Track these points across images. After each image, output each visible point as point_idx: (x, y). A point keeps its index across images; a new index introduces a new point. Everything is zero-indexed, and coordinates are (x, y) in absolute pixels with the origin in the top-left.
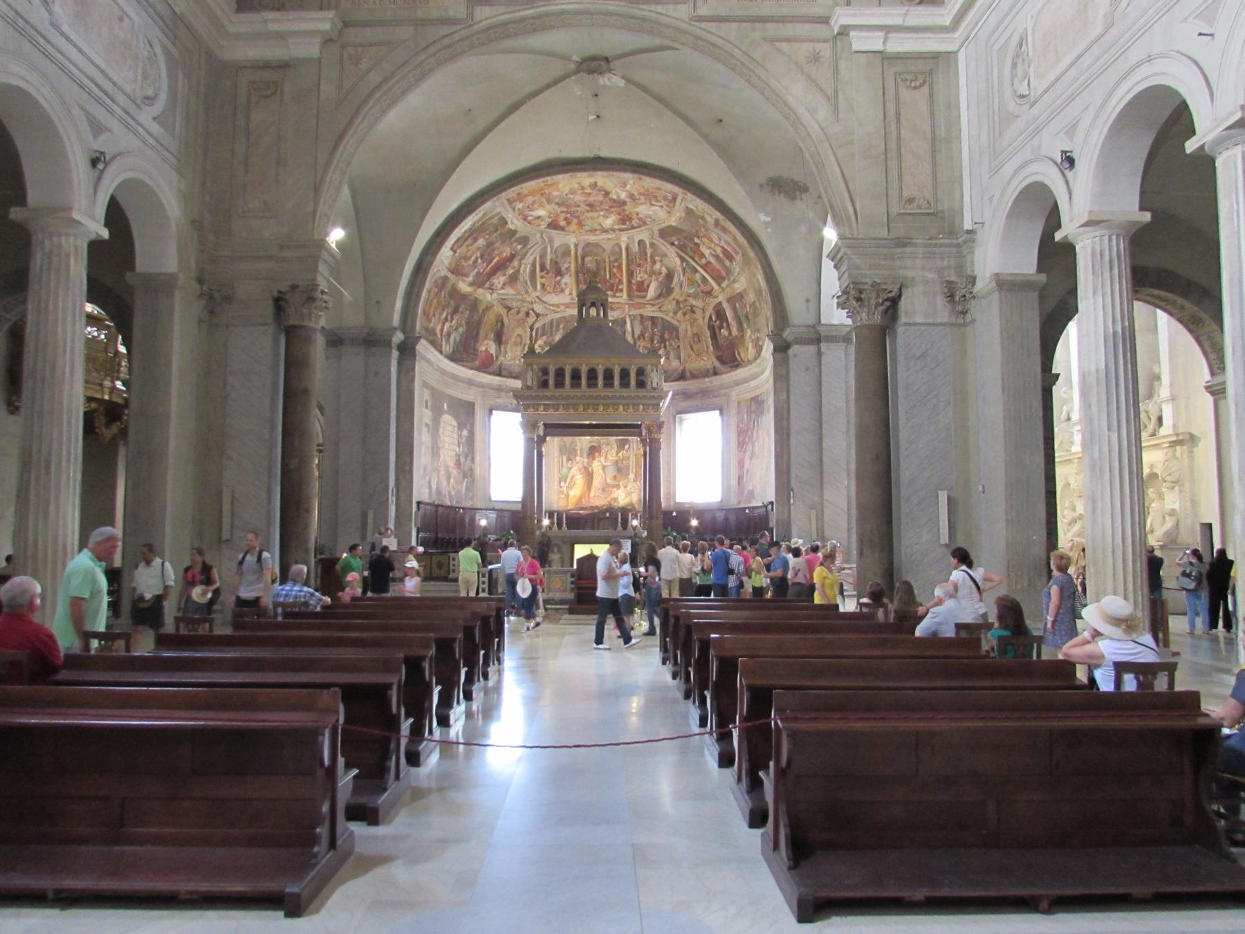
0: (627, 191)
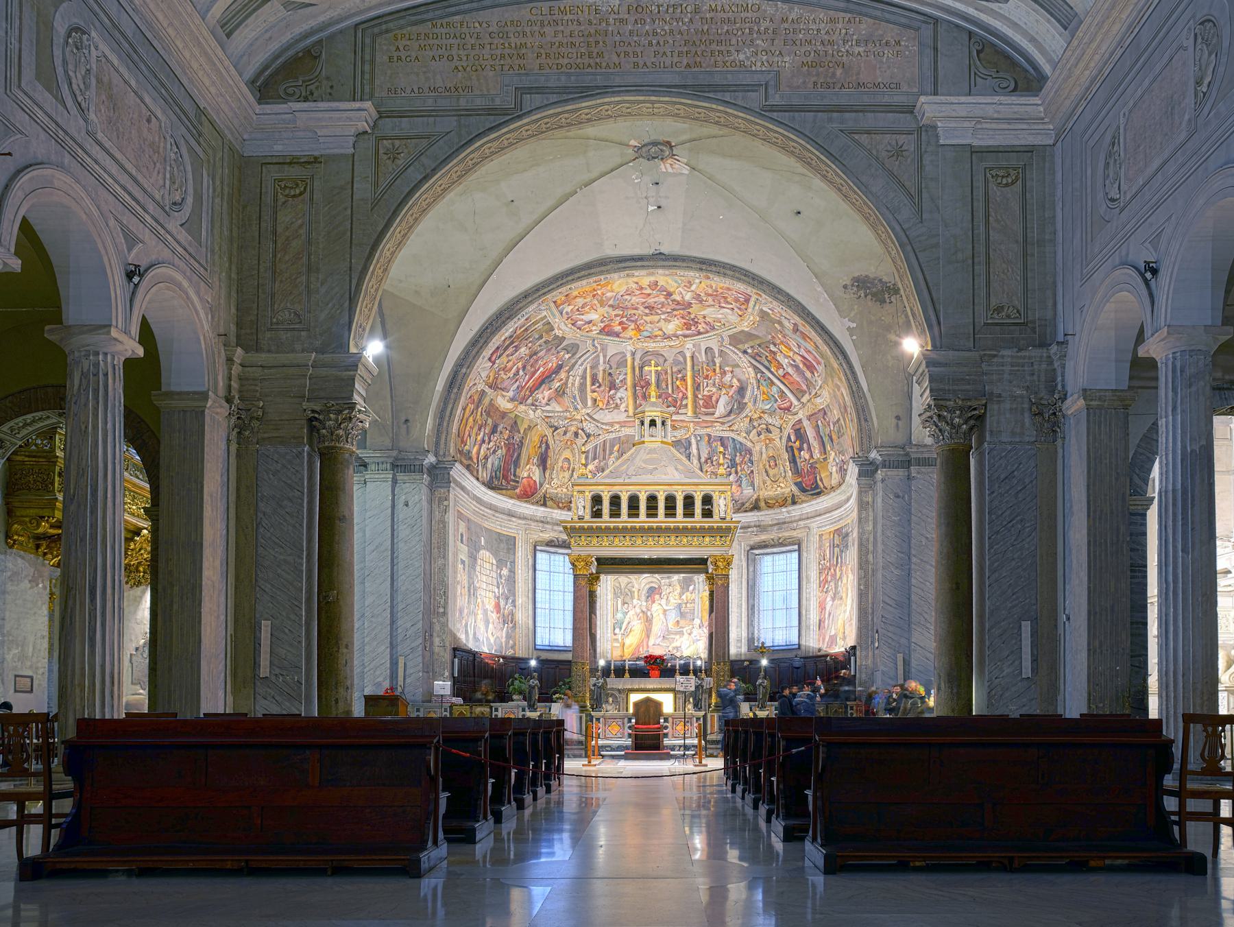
0: (692, 291)
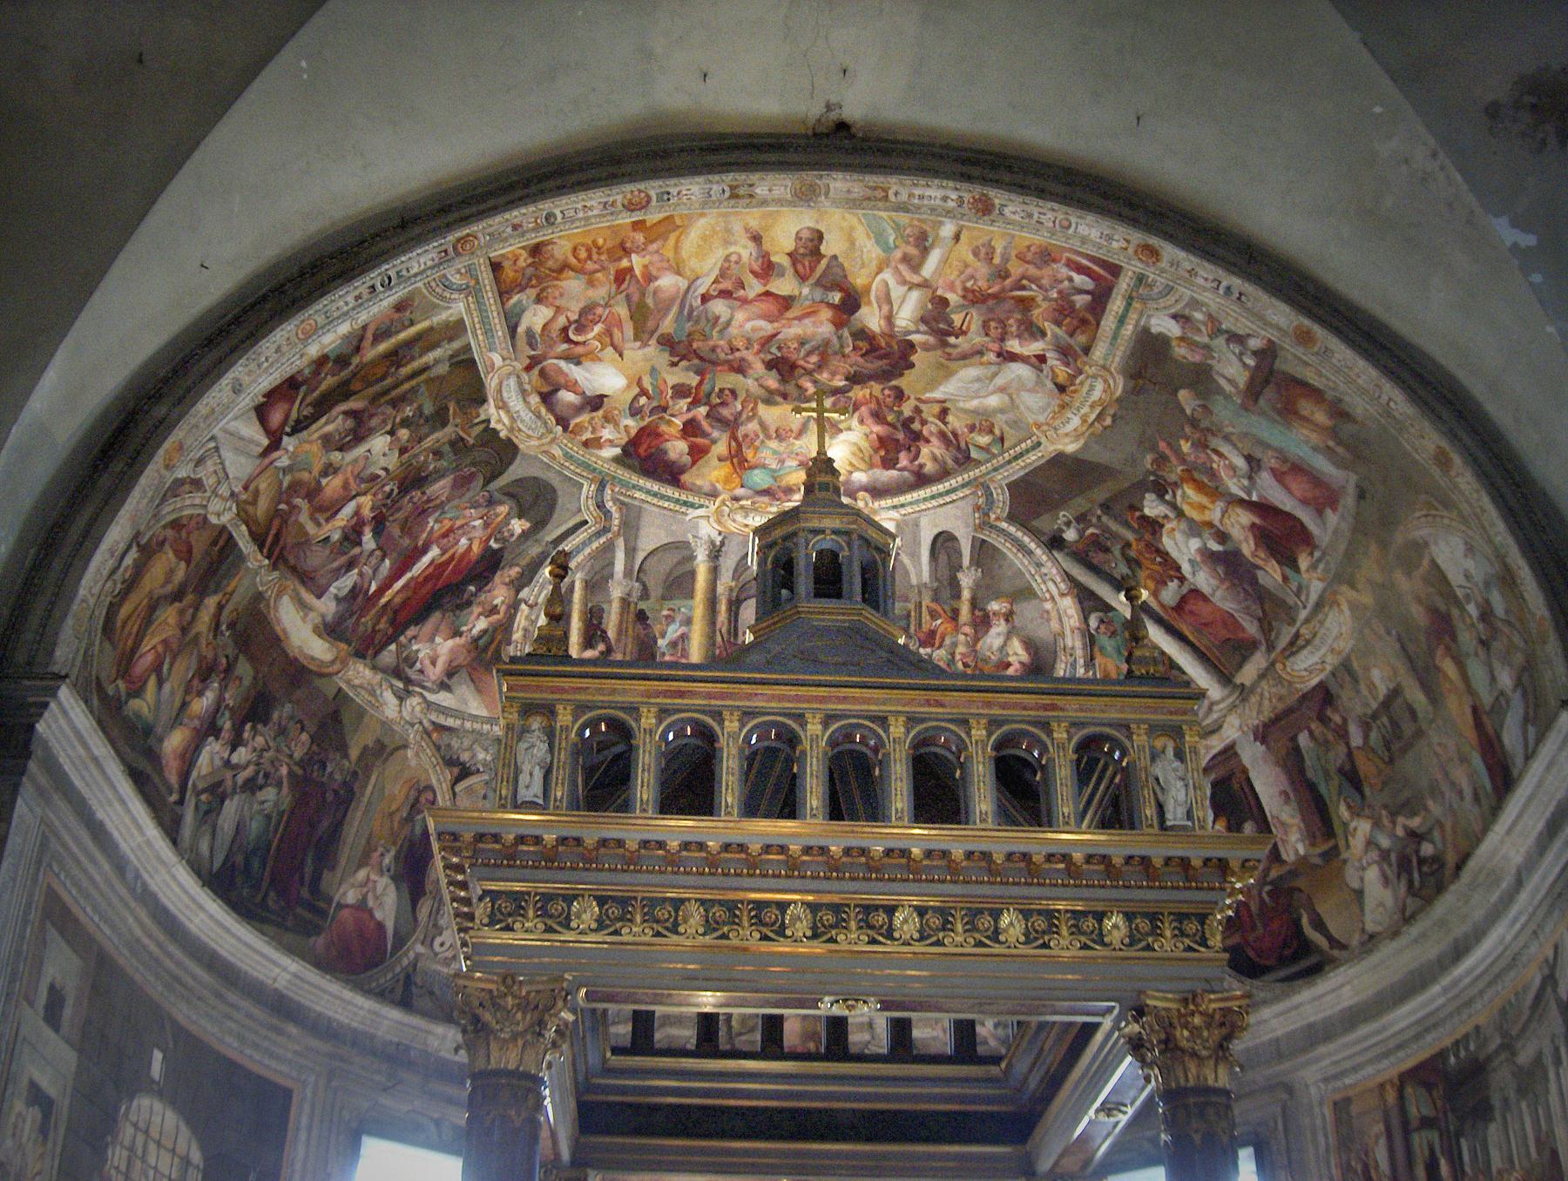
0: (925, 285)
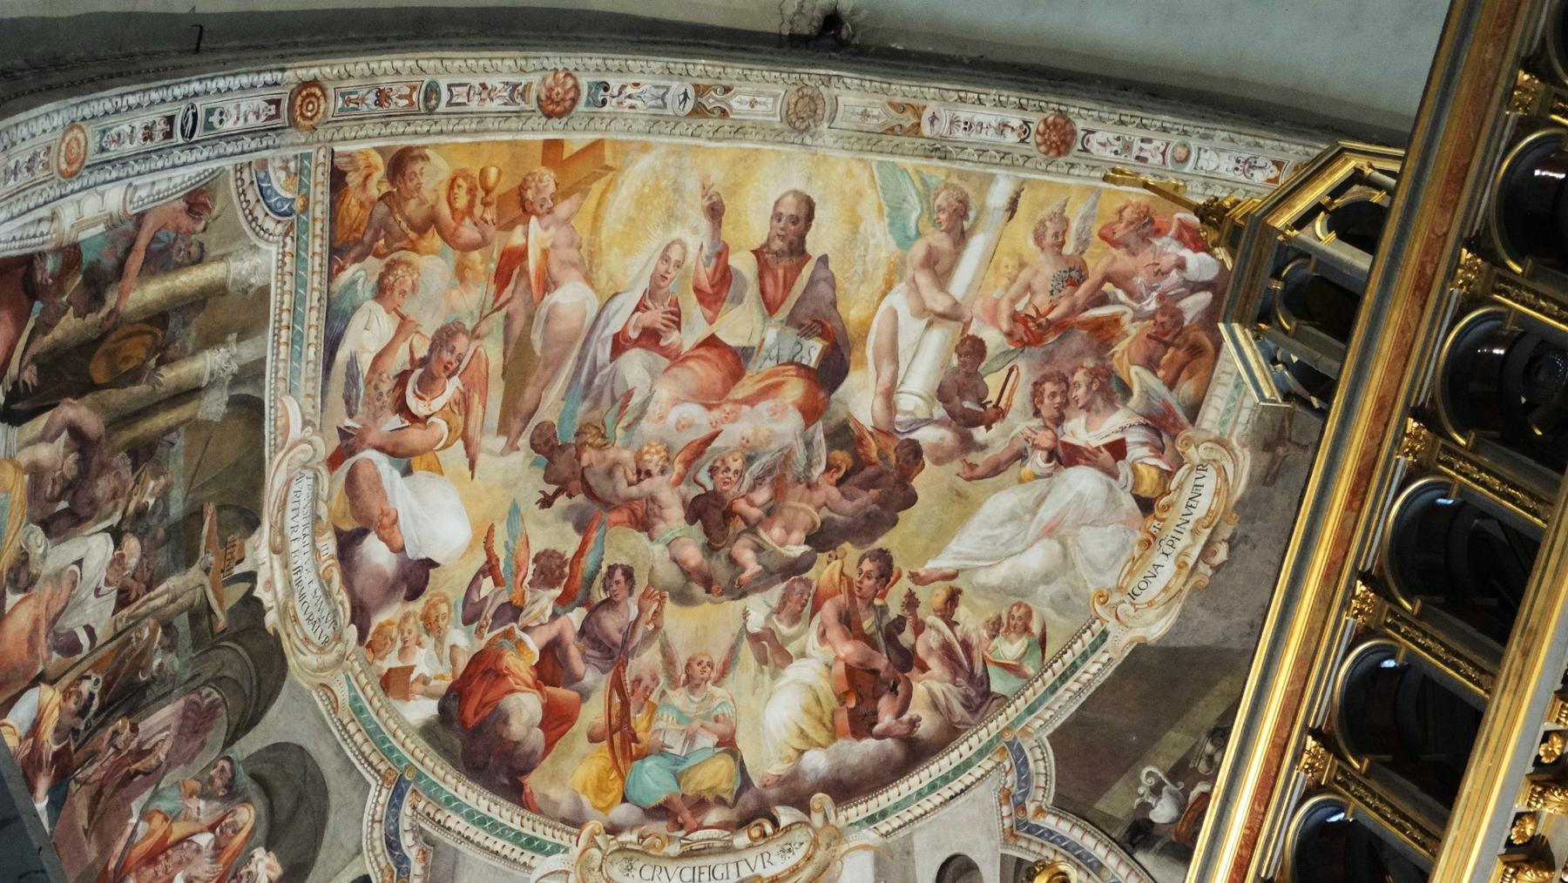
0: (952, 315)
